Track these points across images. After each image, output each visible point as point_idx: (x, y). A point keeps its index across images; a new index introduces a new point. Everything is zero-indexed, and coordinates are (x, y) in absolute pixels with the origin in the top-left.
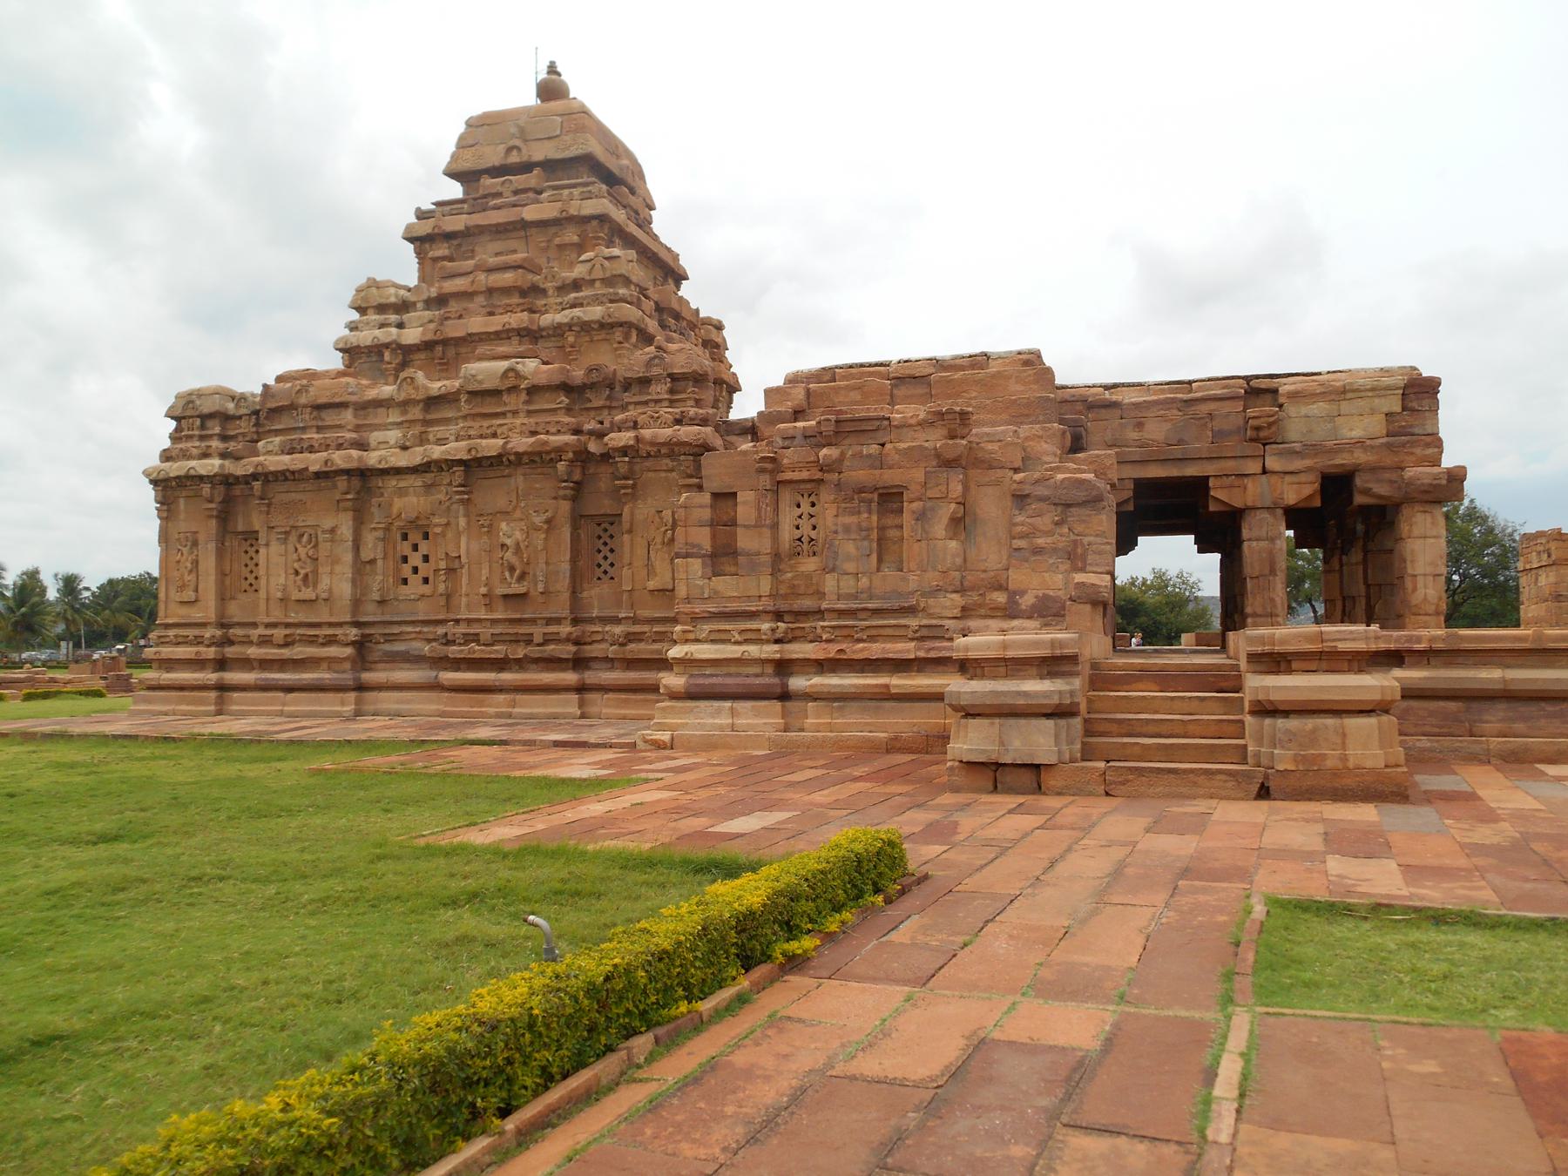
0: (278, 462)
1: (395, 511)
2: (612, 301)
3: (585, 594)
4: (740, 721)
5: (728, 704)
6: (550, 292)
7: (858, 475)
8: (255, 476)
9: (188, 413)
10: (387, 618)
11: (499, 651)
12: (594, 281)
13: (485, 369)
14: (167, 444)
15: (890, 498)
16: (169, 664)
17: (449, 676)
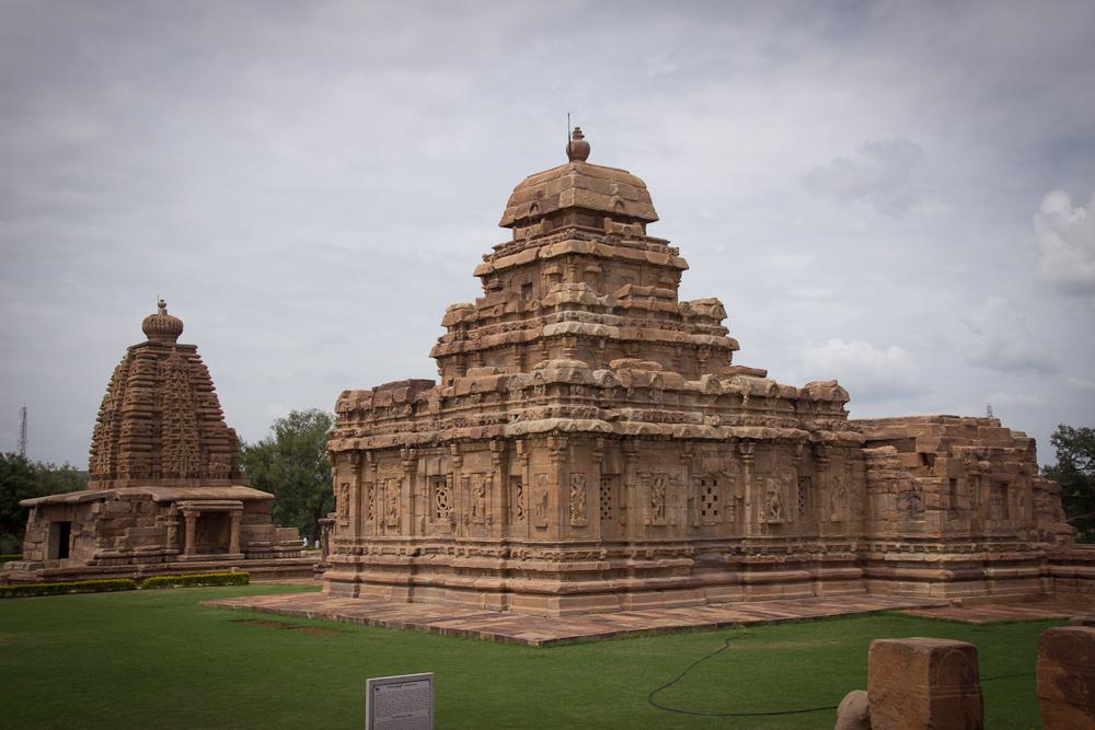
0: (654, 428)
5: (968, 583)
6: (686, 319)
7: (997, 475)
12: (714, 319)
15: (1004, 486)
17: (749, 575)
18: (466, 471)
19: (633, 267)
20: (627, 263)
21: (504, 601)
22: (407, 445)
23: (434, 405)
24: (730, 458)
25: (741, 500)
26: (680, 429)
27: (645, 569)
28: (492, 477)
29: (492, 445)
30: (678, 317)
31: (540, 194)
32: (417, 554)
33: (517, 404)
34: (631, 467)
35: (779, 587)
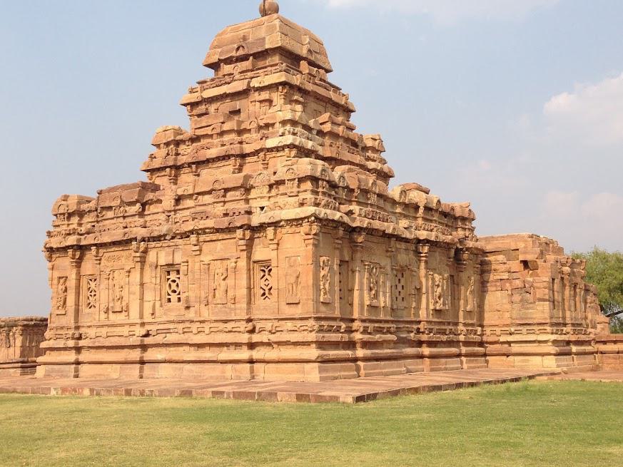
18: (206, 258)
19: (322, 103)
20: (318, 99)
21: (252, 371)
22: (139, 238)
23: (168, 203)
24: (411, 255)
25: (419, 290)
26: (389, 227)
27: (369, 342)
28: (236, 262)
29: (239, 233)
30: (355, 144)
31: (244, 38)
32: (147, 335)
33: (262, 198)
34: (358, 255)
35: (443, 360)
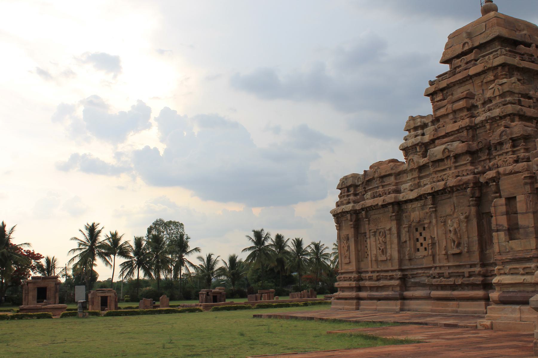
1: (412, 219)
2: (504, 105)
3: (488, 252)
4: (525, 316)
5: (518, 307)
6: (479, 107)
8: (362, 209)
9: (343, 186)
10: (412, 267)
11: (451, 281)
12: (496, 97)
13: (437, 151)
14: (338, 199)
16: (343, 289)
